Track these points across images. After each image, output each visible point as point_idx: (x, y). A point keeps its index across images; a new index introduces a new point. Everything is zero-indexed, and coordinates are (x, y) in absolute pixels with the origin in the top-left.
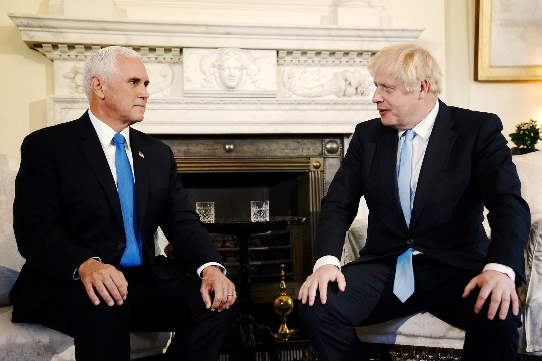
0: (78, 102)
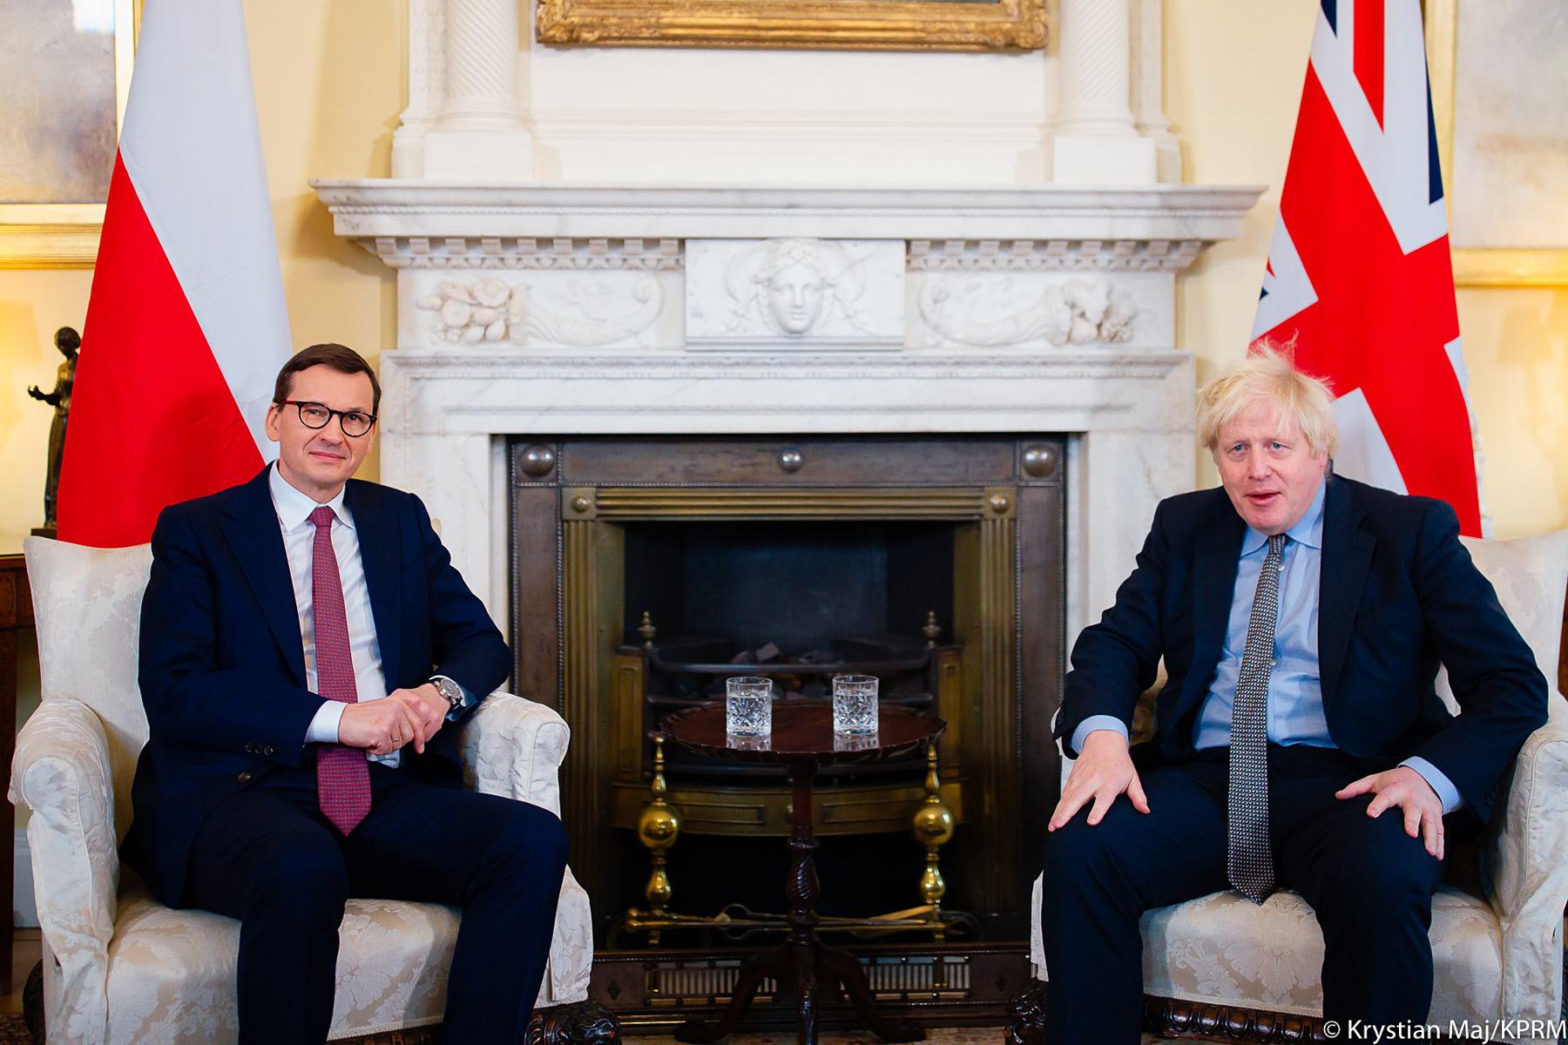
0: (449, 364)
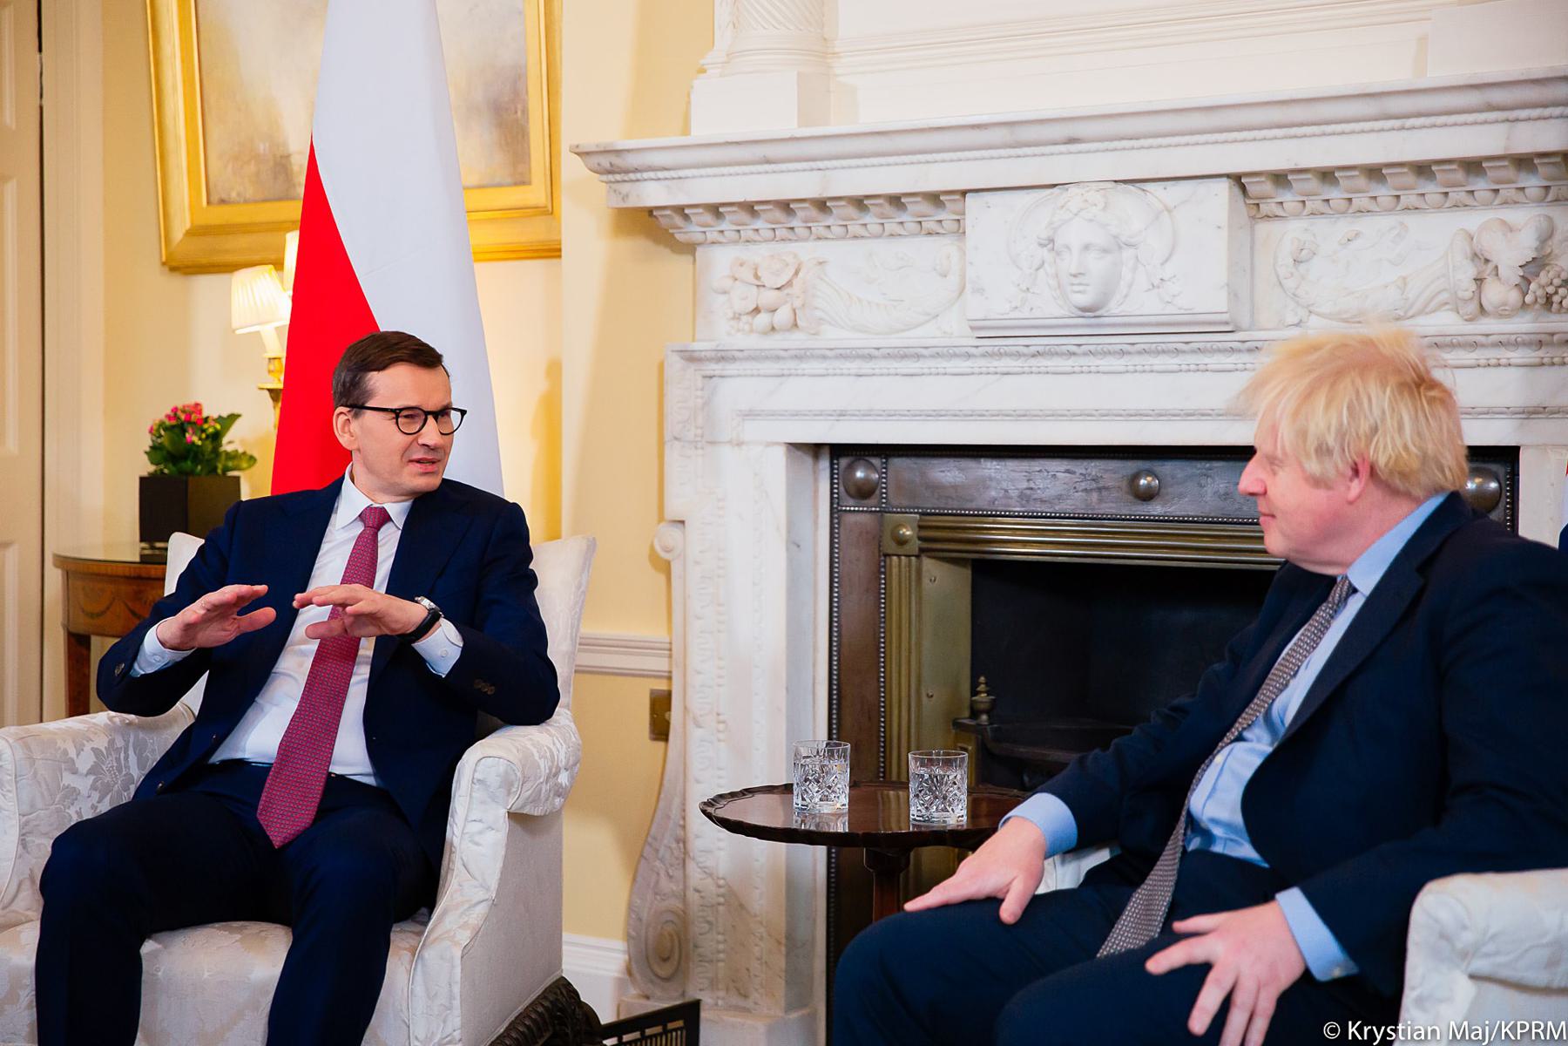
0: (734, 359)
